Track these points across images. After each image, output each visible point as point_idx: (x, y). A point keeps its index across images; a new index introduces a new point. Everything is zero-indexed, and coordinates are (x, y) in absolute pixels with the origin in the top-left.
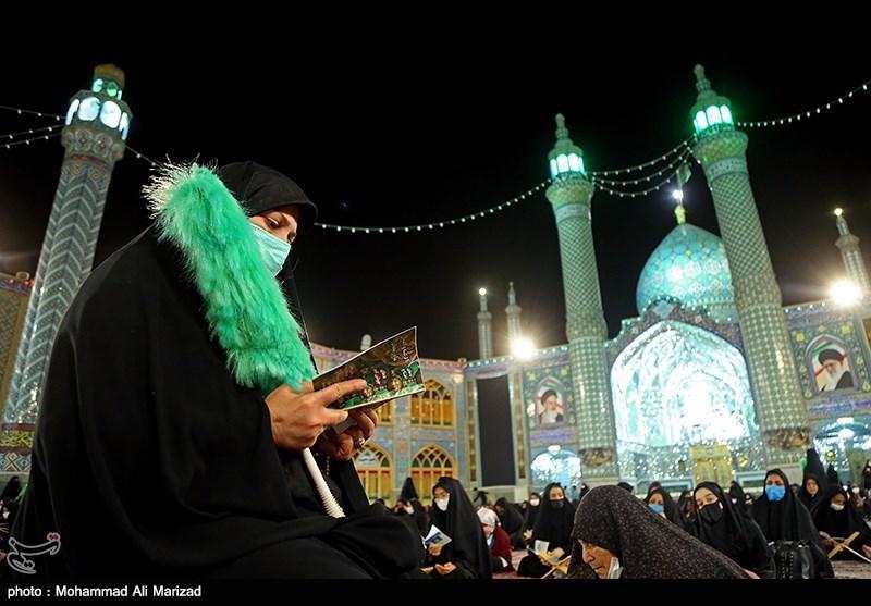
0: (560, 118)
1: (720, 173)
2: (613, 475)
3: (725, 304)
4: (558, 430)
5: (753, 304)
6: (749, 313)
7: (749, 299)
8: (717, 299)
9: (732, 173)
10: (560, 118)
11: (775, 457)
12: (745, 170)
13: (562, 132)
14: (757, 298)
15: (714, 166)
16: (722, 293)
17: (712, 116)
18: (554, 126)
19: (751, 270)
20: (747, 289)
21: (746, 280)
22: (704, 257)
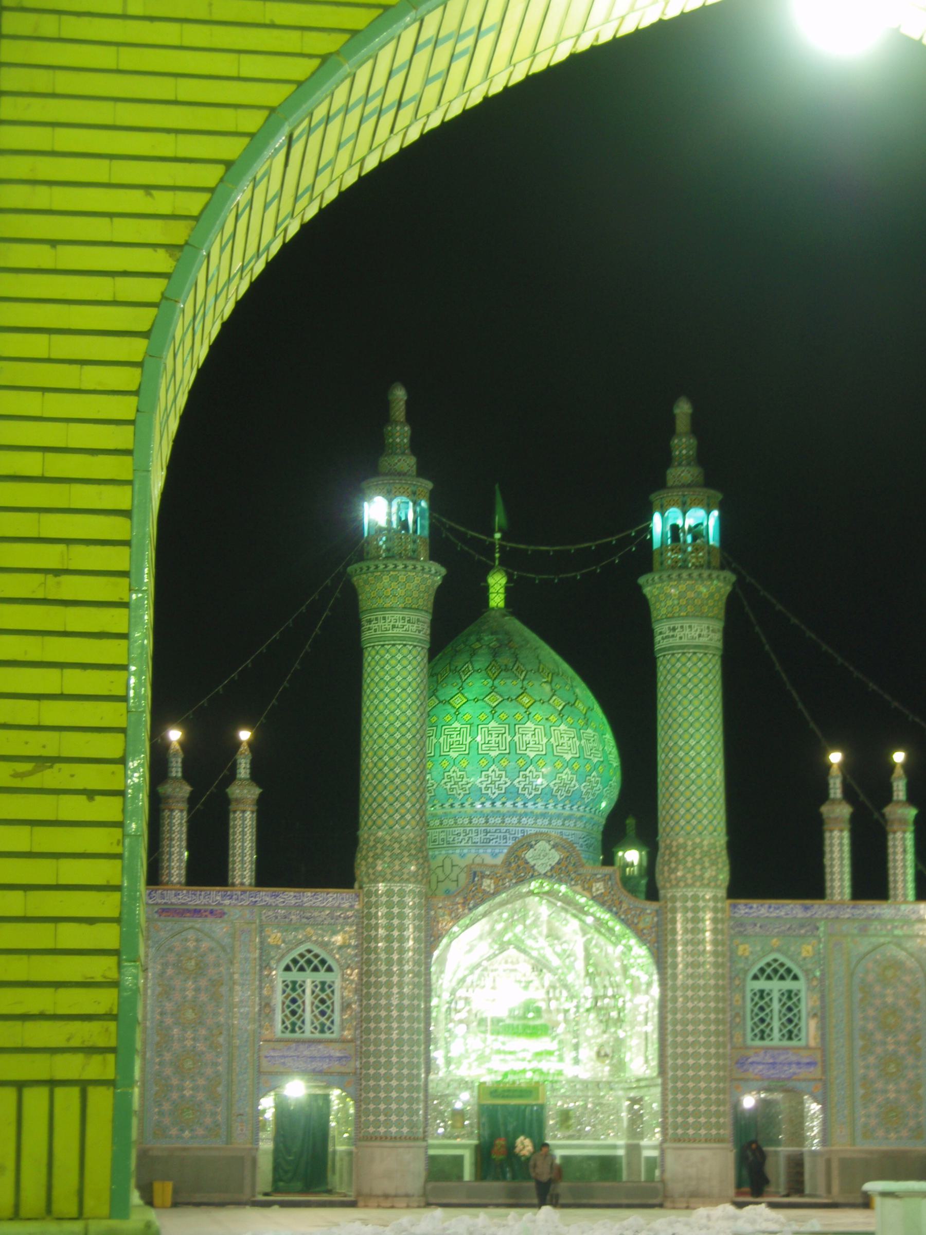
0: (400, 394)
1: (684, 641)
2: (416, 1139)
3: (569, 817)
4: (321, 1047)
5: (693, 885)
6: (685, 899)
7: (689, 876)
8: (560, 806)
9: (707, 647)
10: (400, 394)
11: (680, 1131)
12: (720, 645)
13: (400, 434)
14: (702, 877)
15: (677, 623)
16: (572, 797)
17: (686, 520)
18: (383, 416)
19: (700, 828)
20: (689, 859)
21: (690, 843)
22: (553, 718)
